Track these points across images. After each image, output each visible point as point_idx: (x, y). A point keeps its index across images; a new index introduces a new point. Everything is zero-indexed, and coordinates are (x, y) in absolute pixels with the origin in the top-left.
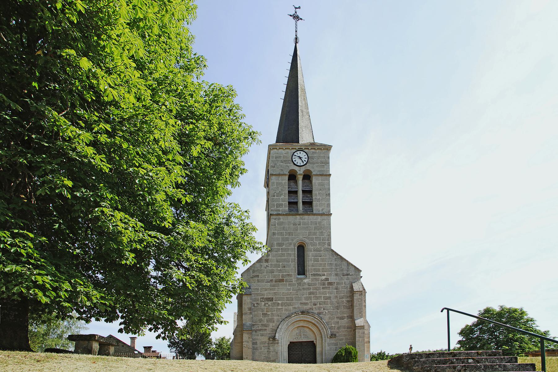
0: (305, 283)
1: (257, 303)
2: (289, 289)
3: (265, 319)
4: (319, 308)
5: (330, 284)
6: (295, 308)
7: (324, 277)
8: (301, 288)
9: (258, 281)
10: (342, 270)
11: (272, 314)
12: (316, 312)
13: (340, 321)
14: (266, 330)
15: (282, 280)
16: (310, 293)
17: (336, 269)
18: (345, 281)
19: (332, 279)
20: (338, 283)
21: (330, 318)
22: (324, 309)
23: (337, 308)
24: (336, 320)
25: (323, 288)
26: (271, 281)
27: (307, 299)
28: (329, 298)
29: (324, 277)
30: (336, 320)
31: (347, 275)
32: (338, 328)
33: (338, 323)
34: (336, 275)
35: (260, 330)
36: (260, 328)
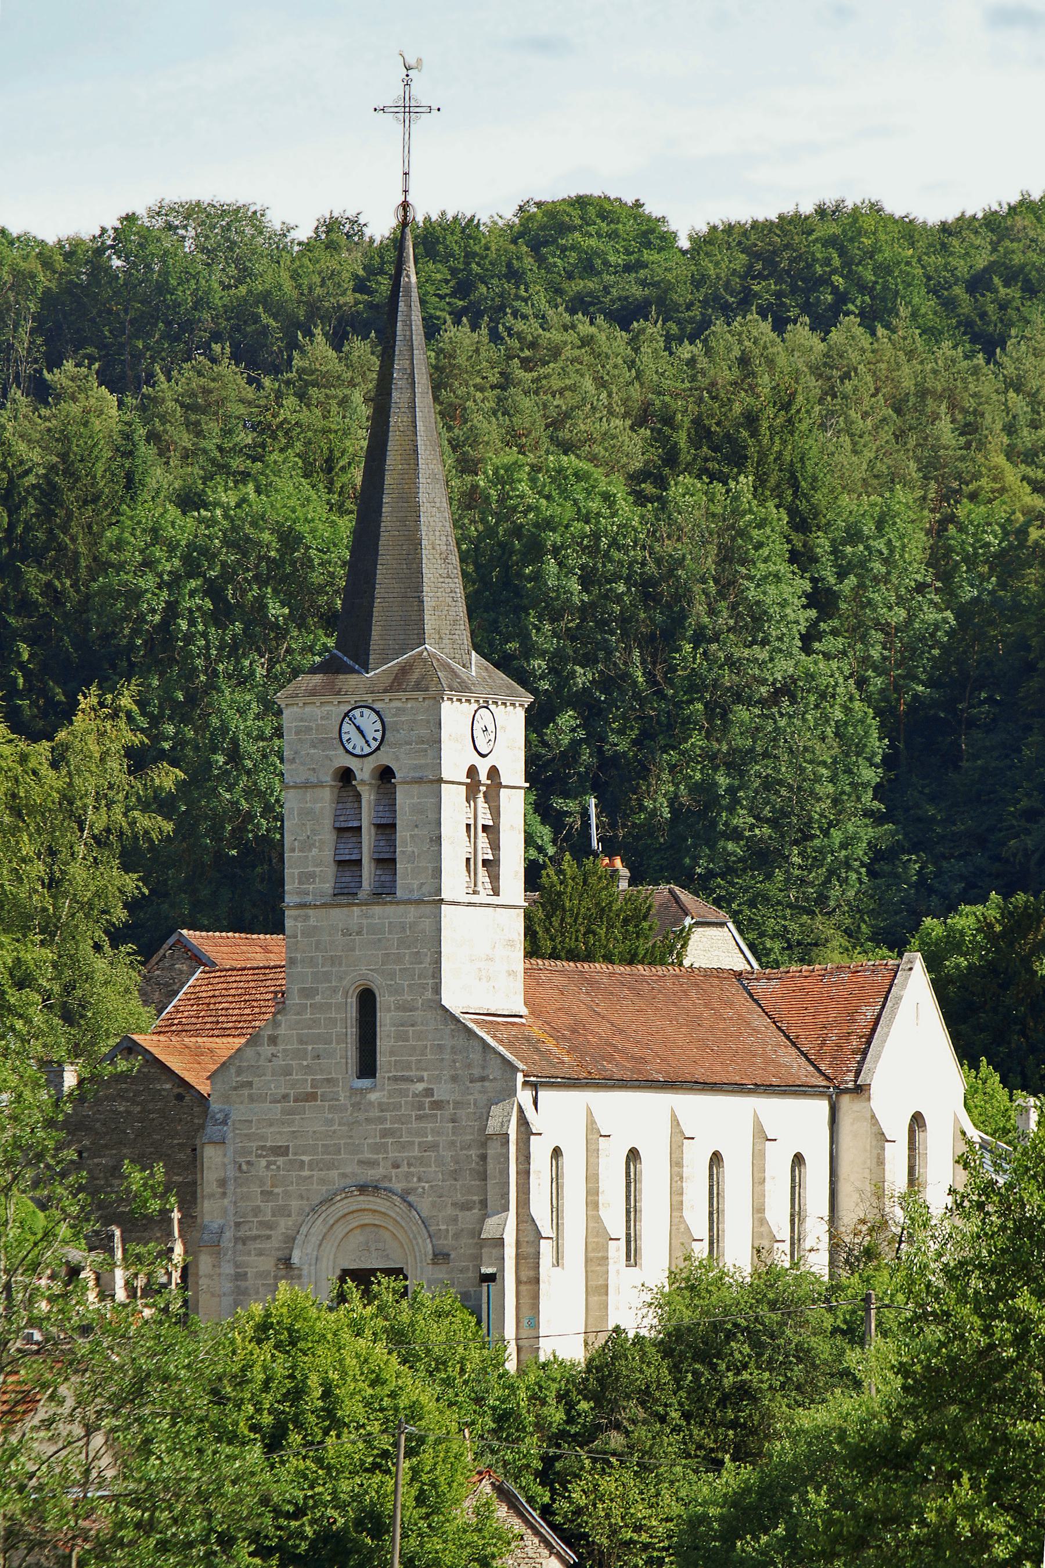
0: (371, 1103)
1: (248, 1163)
2: (330, 1122)
3: (268, 1208)
4: (408, 1176)
5: (437, 1105)
6: (344, 1175)
7: (420, 1087)
8: (362, 1116)
9: (251, 1099)
10: (469, 1066)
11: (286, 1192)
12: (398, 1186)
13: (460, 1214)
14: (269, 1237)
15: (311, 1097)
16: (385, 1133)
17: (454, 1061)
18: (477, 1096)
19: (443, 1091)
20: (457, 1104)
21: (434, 1205)
22: (420, 1180)
23: (455, 1175)
24: (450, 1211)
25: (419, 1118)
26: (285, 1097)
27: (377, 1148)
28: (434, 1146)
29: (420, 1087)
30: (450, 1211)
31: (483, 1079)
32: (457, 1236)
33: (455, 1220)
34: (454, 1079)
35: (255, 1238)
36: (255, 1232)
